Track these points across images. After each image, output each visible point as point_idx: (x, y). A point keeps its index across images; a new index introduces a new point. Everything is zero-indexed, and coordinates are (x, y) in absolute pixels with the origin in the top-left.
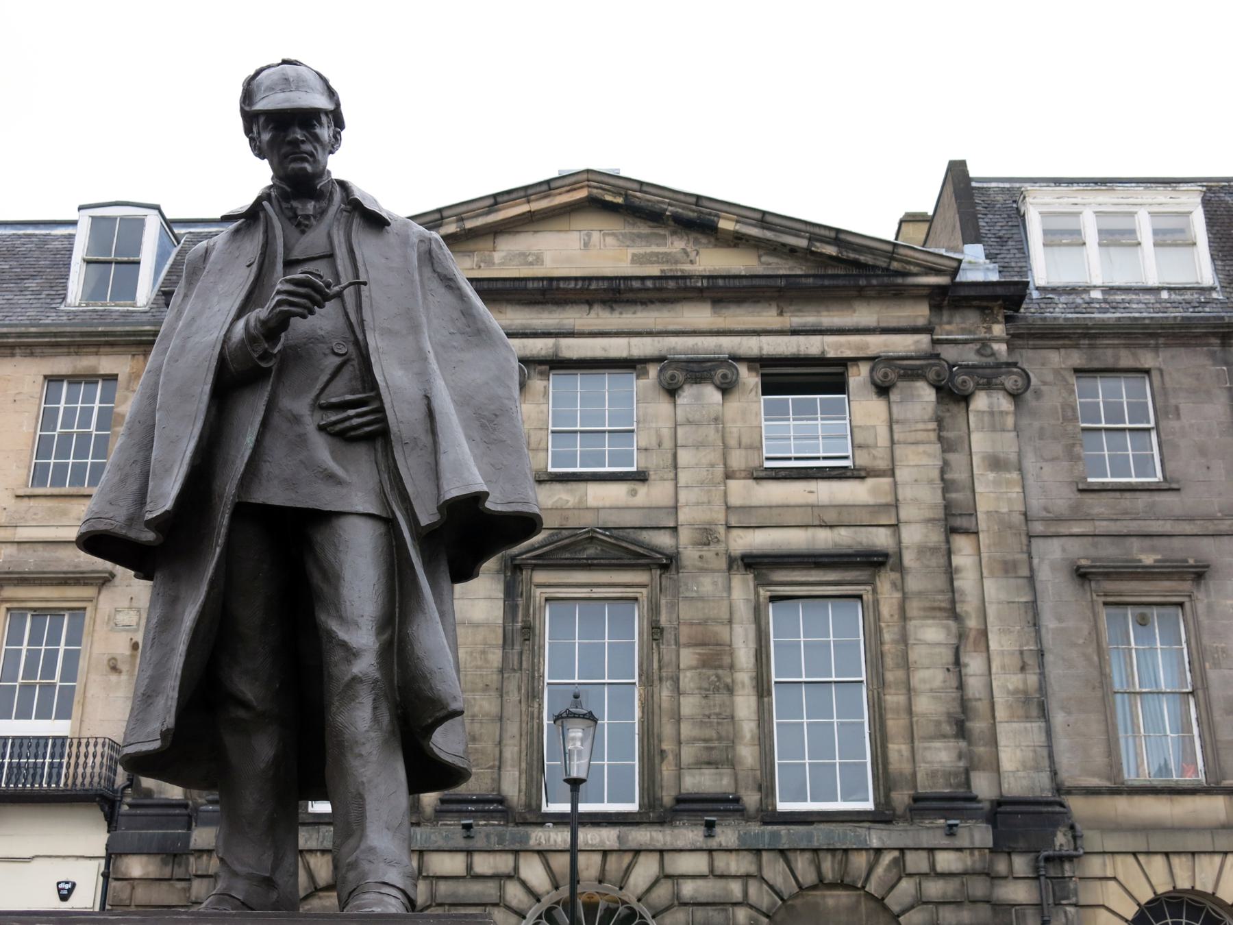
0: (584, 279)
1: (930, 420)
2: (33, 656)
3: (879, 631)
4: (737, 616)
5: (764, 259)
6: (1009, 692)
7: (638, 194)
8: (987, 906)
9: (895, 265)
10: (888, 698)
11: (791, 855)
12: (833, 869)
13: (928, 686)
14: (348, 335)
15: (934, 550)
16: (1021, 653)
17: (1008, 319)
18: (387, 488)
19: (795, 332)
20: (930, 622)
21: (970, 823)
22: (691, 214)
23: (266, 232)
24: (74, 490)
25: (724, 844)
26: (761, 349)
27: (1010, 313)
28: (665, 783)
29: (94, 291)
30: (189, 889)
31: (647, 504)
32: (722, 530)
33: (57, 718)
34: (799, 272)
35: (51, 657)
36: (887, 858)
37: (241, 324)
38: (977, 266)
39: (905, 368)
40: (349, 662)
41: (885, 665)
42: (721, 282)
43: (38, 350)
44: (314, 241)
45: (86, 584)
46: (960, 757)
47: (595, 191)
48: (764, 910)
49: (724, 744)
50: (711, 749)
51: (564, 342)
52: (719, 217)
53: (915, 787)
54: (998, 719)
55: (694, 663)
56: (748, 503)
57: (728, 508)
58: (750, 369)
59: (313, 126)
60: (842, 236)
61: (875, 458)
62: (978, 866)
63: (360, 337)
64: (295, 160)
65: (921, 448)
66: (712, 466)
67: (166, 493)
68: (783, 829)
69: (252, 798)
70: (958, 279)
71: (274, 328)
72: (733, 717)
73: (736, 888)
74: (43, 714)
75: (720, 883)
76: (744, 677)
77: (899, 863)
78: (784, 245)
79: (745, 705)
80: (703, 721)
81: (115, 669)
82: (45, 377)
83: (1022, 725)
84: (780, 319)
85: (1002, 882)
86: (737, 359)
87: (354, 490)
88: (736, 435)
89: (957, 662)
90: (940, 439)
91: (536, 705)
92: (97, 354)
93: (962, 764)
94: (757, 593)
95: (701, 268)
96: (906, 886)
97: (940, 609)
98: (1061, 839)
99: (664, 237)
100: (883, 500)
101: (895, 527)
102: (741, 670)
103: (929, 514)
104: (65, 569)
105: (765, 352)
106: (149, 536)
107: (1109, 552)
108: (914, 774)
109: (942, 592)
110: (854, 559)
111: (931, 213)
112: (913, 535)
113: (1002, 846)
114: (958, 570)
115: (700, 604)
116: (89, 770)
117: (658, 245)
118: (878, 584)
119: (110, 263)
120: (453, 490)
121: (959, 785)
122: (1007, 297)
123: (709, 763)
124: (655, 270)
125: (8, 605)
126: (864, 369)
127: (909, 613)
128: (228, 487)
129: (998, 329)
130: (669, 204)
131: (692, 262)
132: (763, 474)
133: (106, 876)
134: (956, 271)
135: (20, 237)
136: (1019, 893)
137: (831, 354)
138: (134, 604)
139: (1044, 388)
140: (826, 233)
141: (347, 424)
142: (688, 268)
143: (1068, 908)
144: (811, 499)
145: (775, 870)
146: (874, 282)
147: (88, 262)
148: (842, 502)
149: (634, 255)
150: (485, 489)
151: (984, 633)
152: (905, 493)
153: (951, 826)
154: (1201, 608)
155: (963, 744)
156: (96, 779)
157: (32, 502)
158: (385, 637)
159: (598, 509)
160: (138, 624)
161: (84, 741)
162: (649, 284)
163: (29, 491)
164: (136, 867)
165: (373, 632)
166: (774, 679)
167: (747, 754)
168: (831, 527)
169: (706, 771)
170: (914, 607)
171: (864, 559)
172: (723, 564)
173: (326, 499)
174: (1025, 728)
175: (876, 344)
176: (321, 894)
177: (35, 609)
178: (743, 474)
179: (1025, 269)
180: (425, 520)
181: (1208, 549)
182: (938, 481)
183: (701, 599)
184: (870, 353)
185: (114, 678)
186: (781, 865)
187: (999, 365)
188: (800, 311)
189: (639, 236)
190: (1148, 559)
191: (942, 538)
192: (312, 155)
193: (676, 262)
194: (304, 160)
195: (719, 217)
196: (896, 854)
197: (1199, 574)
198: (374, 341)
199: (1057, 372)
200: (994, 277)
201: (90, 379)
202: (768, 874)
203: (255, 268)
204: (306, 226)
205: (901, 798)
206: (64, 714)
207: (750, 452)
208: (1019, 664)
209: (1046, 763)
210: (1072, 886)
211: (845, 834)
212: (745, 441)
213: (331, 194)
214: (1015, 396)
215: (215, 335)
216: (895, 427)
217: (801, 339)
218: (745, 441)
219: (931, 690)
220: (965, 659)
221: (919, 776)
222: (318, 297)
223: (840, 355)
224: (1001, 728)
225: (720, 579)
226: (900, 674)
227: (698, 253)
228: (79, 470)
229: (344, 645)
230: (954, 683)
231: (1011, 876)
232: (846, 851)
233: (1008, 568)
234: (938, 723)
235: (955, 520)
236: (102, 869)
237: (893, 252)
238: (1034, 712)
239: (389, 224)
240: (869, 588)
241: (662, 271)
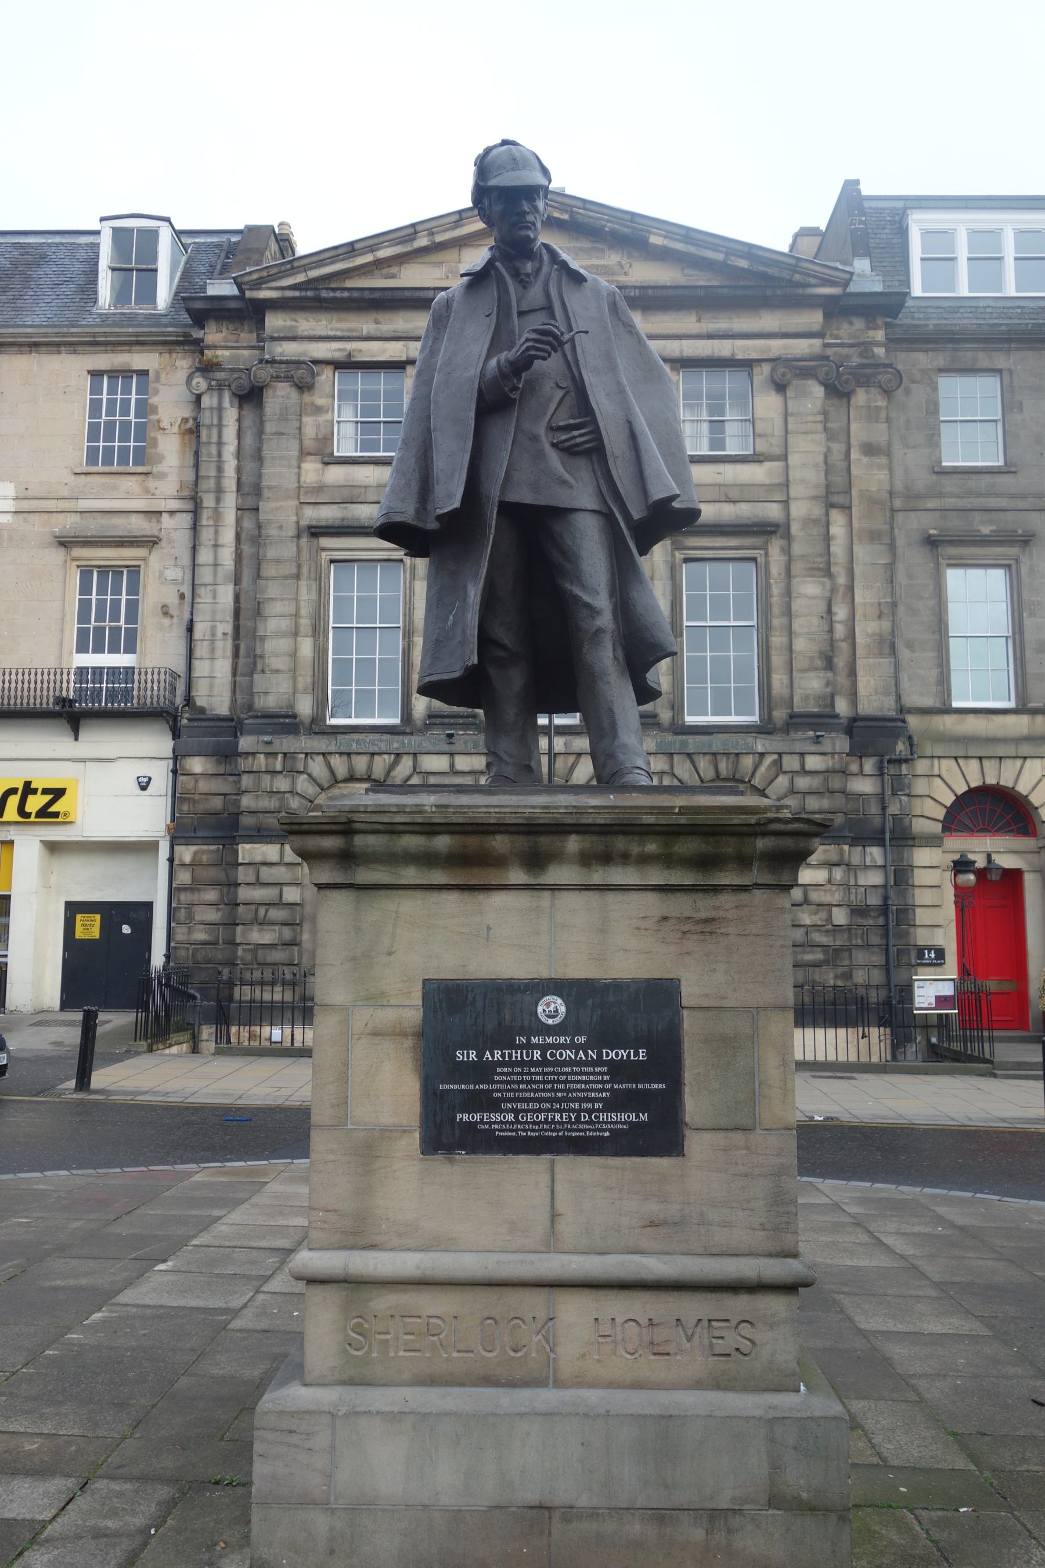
1: (819, 413)
2: (101, 604)
3: (768, 586)
4: (657, 575)
5: (686, 271)
6: (867, 635)
7: (581, 211)
8: (843, 795)
9: (797, 277)
10: (774, 639)
11: (695, 758)
12: (727, 768)
13: (805, 630)
14: (567, 372)
15: (815, 522)
16: (879, 604)
17: (887, 326)
18: (604, 490)
19: (710, 336)
20: (810, 579)
21: (833, 735)
23: (498, 287)
24: (121, 469)
26: (682, 351)
27: (889, 320)
29: (121, 295)
30: (239, 782)
33: (125, 652)
34: (716, 283)
35: (116, 604)
36: (768, 760)
37: (493, 362)
38: (865, 276)
39: (800, 368)
40: (593, 618)
41: (772, 613)
42: (650, 292)
43: (80, 348)
44: (535, 295)
45: (138, 546)
46: (828, 684)
52: (650, 232)
53: (792, 707)
54: (858, 656)
58: (672, 369)
59: (534, 200)
61: (771, 445)
62: (837, 767)
63: (576, 374)
64: (522, 228)
65: (810, 437)
67: (450, 496)
68: (690, 739)
69: (510, 713)
70: (848, 290)
71: (520, 366)
74: (114, 649)
77: (778, 764)
78: (704, 258)
81: (166, 614)
82: (89, 372)
83: (877, 660)
84: (698, 324)
85: (855, 778)
87: (580, 493)
89: (829, 611)
90: (825, 429)
92: (129, 351)
93: (829, 690)
94: (673, 556)
95: (633, 279)
96: (782, 781)
97: (818, 569)
98: (901, 747)
99: (602, 251)
100: (776, 481)
101: (786, 503)
103: (813, 492)
104: (121, 534)
106: (432, 525)
107: (955, 523)
108: (792, 697)
109: (821, 555)
110: (751, 529)
111: (823, 228)
112: (799, 510)
113: (858, 751)
114: (834, 538)
116: (155, 693)
117: (597, 258)
118: (770, 549)
119: (132, 270)
120: (657, 494)
121: (825, 706)
122: (887, 307)
125: (78, 563)
126: (766, 368)
127: (793, 573)
128: (493, 491)
129: (880, 335)
130: (608, 221)
131: (626, 274)
133: (175, 772)
134: (847, 283)
135: (49, 245)
136: (864, 786)
137: (740, 357)
138: (179, 563)
139: (912, 385)
140: (741, 248)
141: (573, 442)
143: (903, 798)
144: (719, 479)
146: (779, 292)
147: (113, 270)
148: (744, 482)
150: (678, 492)
151: (851, 588)
152: (794, 475)
153: (818, 737)
154: (1024, 570)
155: (830, 674)
156: (162, 700)
157: (89, 479)
158: (614, 600)
160: (183, 579)
161: (143, 671)
163: (85, 469)
164: (197, 765)
165: (607, 597)
166: (686, 623)
168: (734, 502)
170: (797, 567)
171: (759, 529)
173: (562, 499)
174: (879, 663)
175: (776, 347)
176: (340, 785)
177: (99, 567)
179: (907, 282)
180: (636, 515)
181: (1036, 521)
182: (822, 465)
184: (772, 355)
185: (166, 621)
186: (688, 765)
187: (877, 366)
188: (715, 318)
189: (581, 249)
190: (986, 530)
191: (823, 511)
192: (534, 224)
194: (529, 228)
195: (650, 232)
196: (776, 757)
197: (1025, 541)
198: (589, 378)
199: (923, 372)
200: (878, 288)
201: (126, 373)
202: (677, 771)
203: (494, 317)
204: (527, 282)
205: (780, 715)
206: (131, 649)
208: (878, 613)
209: (894, 690)
210: (906, 781)
211: (737, 743)
213: (541, 255)
214: (888, 393)
215: (472, 372)
216: (790, 419)
217: (716, 342)
219: (808, 633)
220: (835, 609)
221: (796, 699)
222: (556, 344)
223: (747, 357)
224: (860, 663)
226: (784, 620)
228: (124, 451)
229: (588, 606)
230: (826, 629)
231: (861, 773)
232: (737, 754)
233: (874, 536)
234: (812, 658)
235: (835, 496)
236: (171, 767)
237: (796, 266)
238: (887, 651)
239: (586, 281)
240: (762, 552)
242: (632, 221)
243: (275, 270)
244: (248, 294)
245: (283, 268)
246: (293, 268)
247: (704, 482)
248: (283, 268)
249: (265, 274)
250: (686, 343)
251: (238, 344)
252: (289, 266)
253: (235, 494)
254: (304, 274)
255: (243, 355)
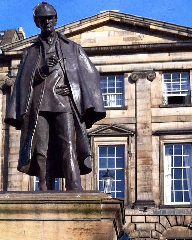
0: (108, 46)
4: (154, 150)
12: (181, 220)
19: (174, 61)
22: (142, 24)
25: (149, 214)
26: (163, 67)
28: (132, 197)
31: (127, 117)
32: (150, 123)
47: (111, 18)
48: (161, 232)
49: (150, 186)
50: (145, 188)
51: (102, 67)
55: (141, 163)
56: (158, 115)
57: (152, 117)
58: (159, 73)
60: (189, 30)
66: (147, 104)
68: (166, 210)
72: (152, 179)
73: (152, 226)
75: (148, 225)
76: (156, 167)
78: (171, 33)
79: (155, 175)
80: (144, 180)
84: (169, 57)
86: (155, 70)
88: (155, 95)
91: (96, 176)
95: (145, 42)
102: (155, 165)
105: (164, 68)
115: (143, 146)
117: (131, 35)
123: (145, 192)
124: (130, 43)
130: (135, 21)
132: (162, 106)
137: (185, 68)
142: (140, 42)
144: (178, 114)
145: (164, 221)
149: (124, 38)
159: (113, 118)
162: (128, 47)
167: (156, 189)
169: (144, 194)
172: (150, 134)
178: (157, 106)
183: (143, 144)
193: (137, 40)
207: (159, 99)
212: (158, 96)
218: (158, 96)
223: (187, 68)
225: (149, 138)
227: (144, 37)
232: (184, 216)
241: (132, 43)
242: (143, 21)
243: (15, 44)
244: (6, 53)
245: (18, 44)
246: (21, 43)
247: (171, 115)
248: (18, 44)
249: (11, 46)
250: (164, 63)
251: (2, 71)
252: (20, 43)
253: (1, 124)
254: (25, 45)
255: (4, 75)
